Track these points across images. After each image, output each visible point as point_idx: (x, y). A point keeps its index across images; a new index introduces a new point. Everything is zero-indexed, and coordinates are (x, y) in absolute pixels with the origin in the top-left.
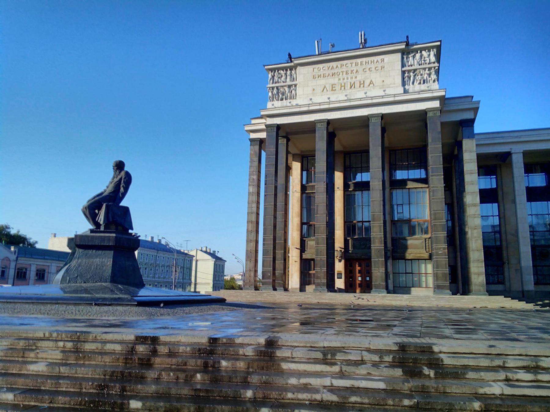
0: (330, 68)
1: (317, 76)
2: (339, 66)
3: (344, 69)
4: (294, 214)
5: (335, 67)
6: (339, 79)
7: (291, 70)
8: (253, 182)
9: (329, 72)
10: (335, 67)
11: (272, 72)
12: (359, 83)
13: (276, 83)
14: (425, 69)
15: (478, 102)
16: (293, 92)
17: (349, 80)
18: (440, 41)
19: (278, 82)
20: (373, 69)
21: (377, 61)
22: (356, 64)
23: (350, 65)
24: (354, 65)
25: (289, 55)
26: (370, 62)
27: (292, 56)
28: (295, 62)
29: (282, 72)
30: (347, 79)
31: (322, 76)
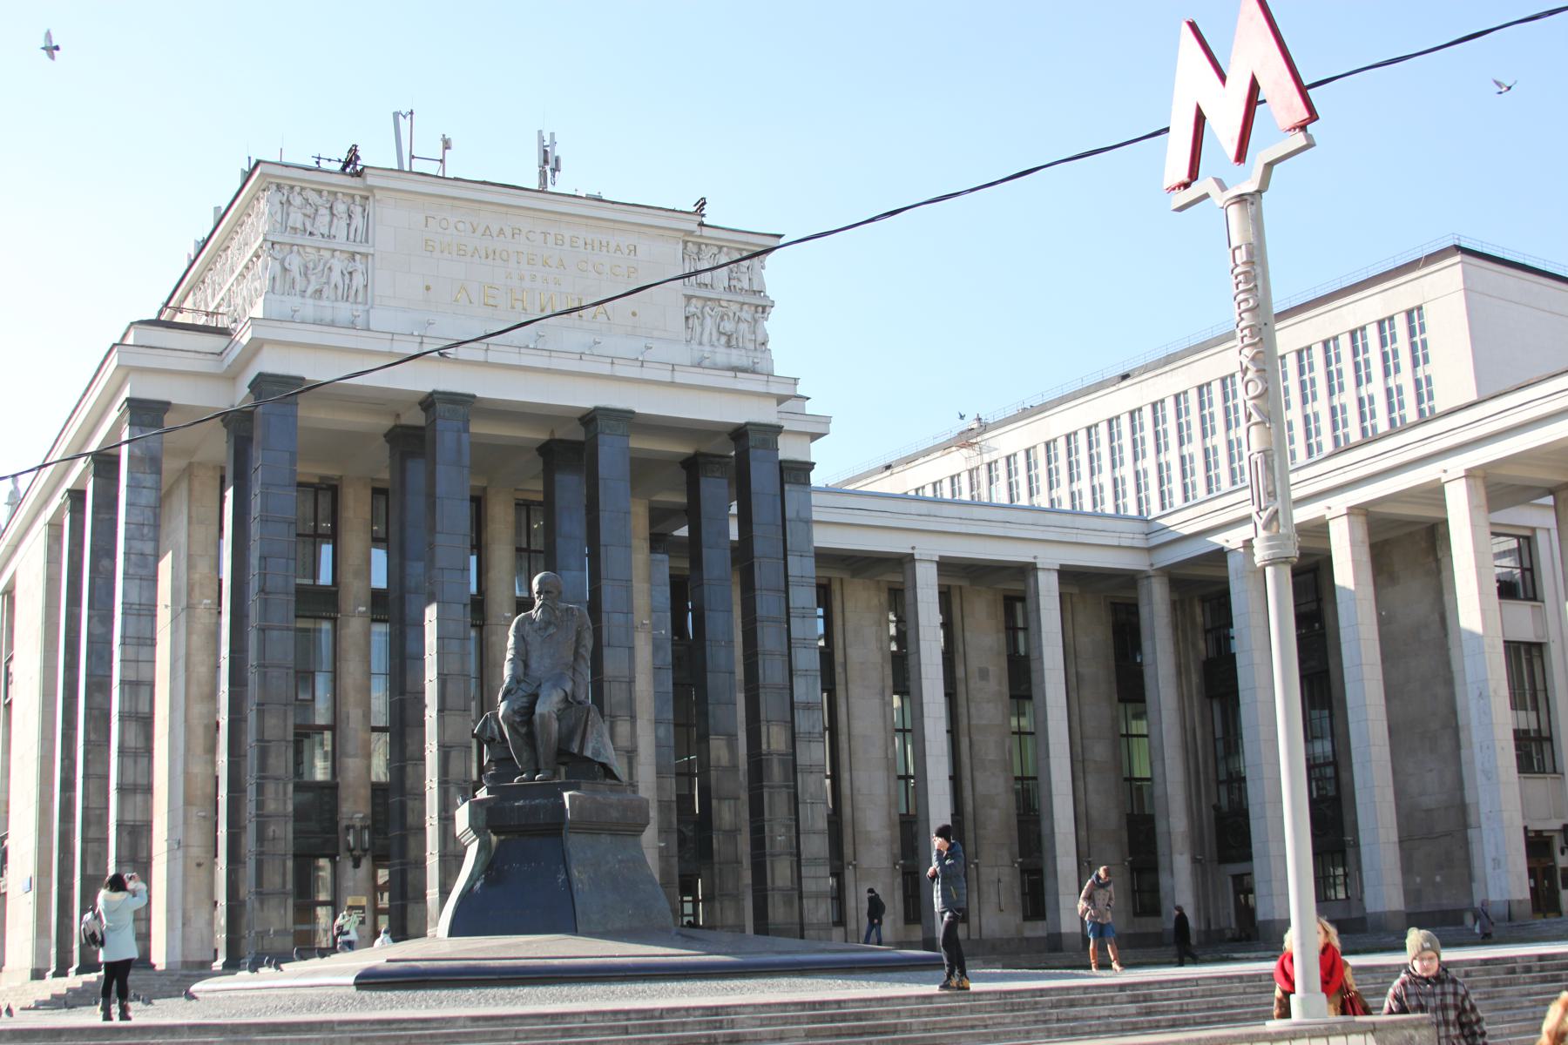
0: (481, 229)
2: (508, 232)
4: (194, 690)
5: (495, 231)
8: (145, 566)
10: (495, 231)
11: (279, 187)
15: (826, 420)
16: (358, 280)
21: (618, 248)
24: (551, 239)
25: (354, 151)
26: (597, 244)
27: (365, 160)
28: (370, 181)
29: (313, 197)
30: (533, 278)
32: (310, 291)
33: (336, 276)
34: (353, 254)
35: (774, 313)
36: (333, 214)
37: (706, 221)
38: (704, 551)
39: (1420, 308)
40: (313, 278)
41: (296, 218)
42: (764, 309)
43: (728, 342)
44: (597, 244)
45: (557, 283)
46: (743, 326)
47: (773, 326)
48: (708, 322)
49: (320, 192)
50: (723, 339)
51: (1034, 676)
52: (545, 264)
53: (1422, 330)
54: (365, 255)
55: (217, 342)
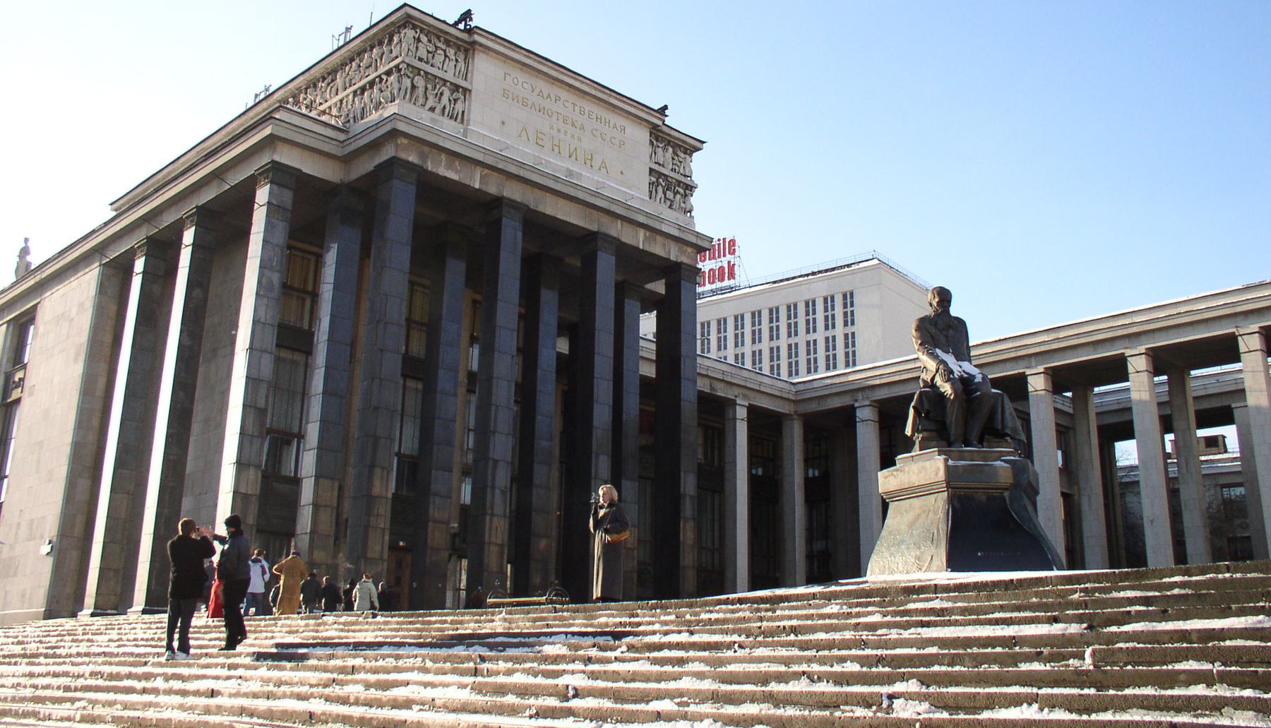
0: (537, 91)
6: (551, 128)
13: (421, 60)
14: (679, 182)
16: (459, 107)
19: (427, 63)
22: (582, 112)
23: (571, 107)
24: (577, 109)
28: (476, 37)
29: (434, 40)
32: (427, 107)
33: (445, 100)
34: (456, 88)
35: (696, 193)
36: (446, 56)
38: (625, 350)
39: (852, 294)
41: (422, 53)
42: (690, 188)
43: (670, 207)
45: (580, 139)
46: (678, 196)
47: (695, 200)
48: (660, 189)
49: (438, 38)
50: (668, 203)
51: (728, 475)
52: (573, 125)
53: (852, 305)
54: (466, 91)
55: (342, 137)
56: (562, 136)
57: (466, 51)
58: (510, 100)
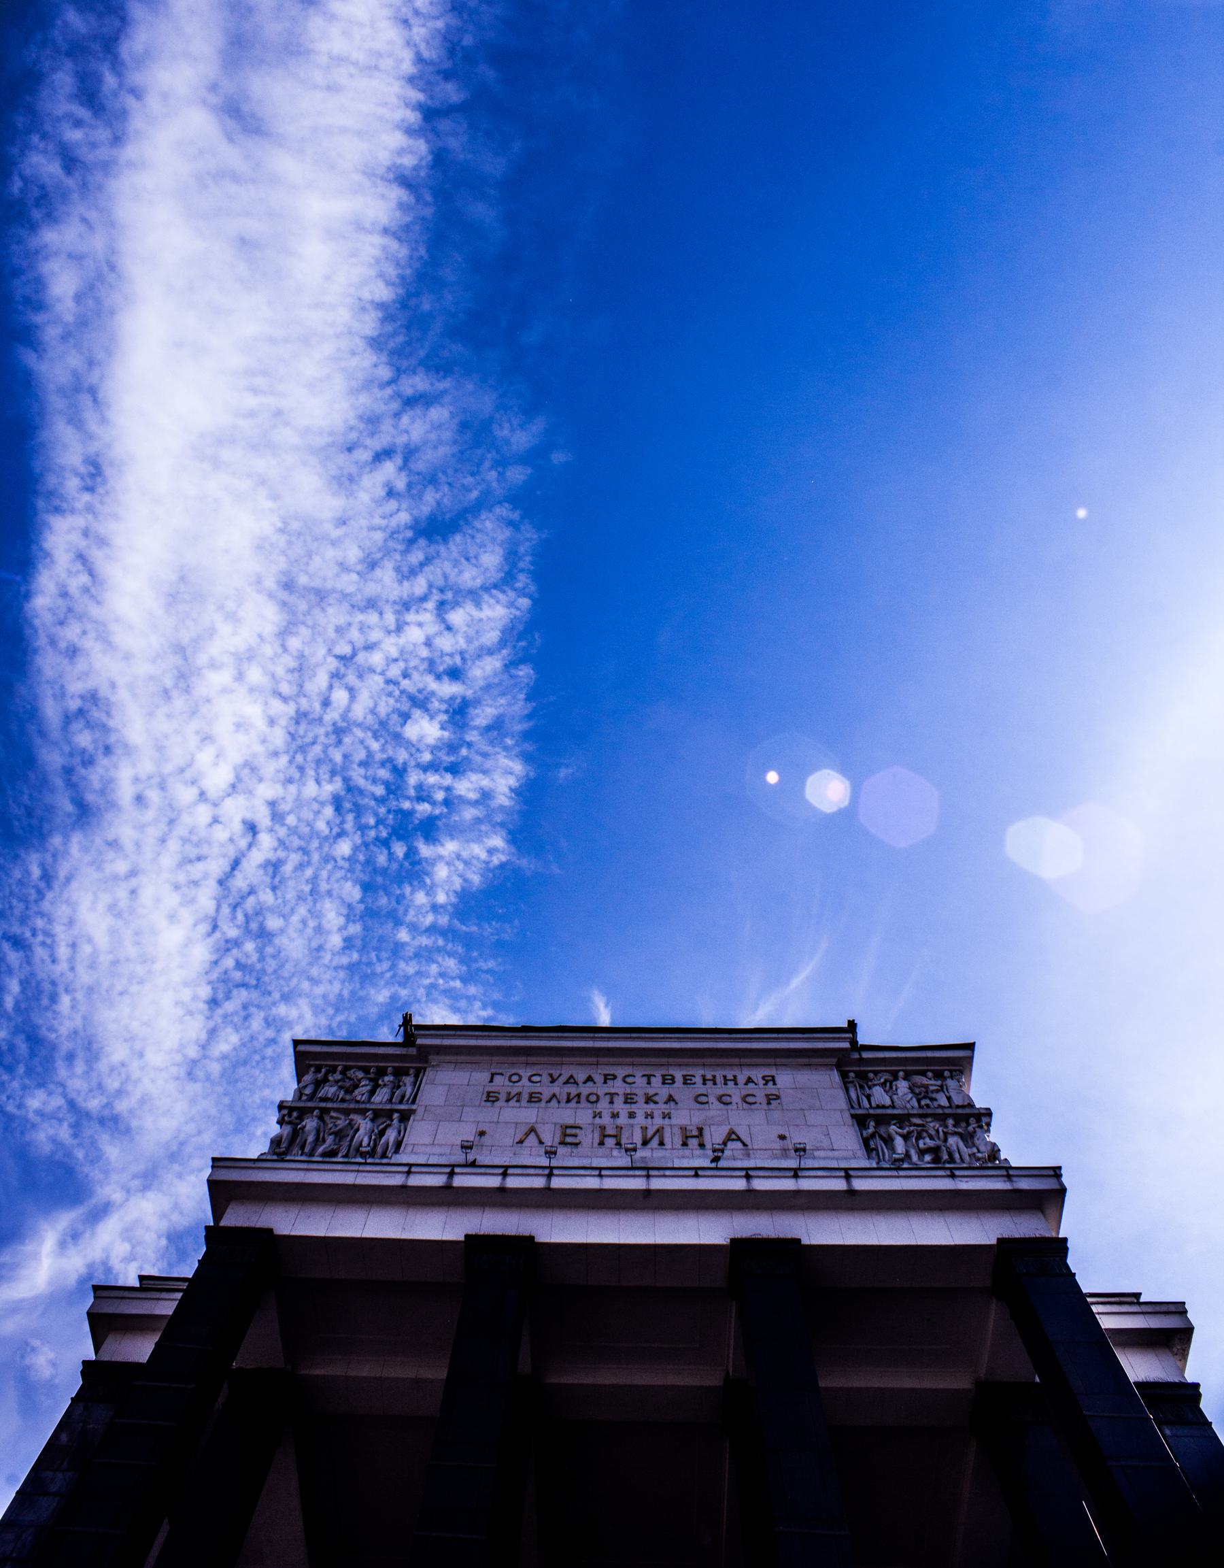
1: (503, 1097)
3: (618, 1087)
5: (581, 1076)
7: (399, 1073)
9: (556, 1089)
11: (318, 1070)
12: (677, 1131)
16: (391, 1135)
17: (640, 1119)
18: (970, 1047)
20: (736, 1098)
23: (640, 1081)
24: (657, 1081)
26: (719, 1080)
30: (632, 1115)
31: (525, 1097)
37: (863, 1039)
40: (330, 1140)
44: (719, 1080)
45: (667, 1116)
49: (366, 1070)
56: (623, 1120)
57: (419, 1073)
58: (501, 1103)
